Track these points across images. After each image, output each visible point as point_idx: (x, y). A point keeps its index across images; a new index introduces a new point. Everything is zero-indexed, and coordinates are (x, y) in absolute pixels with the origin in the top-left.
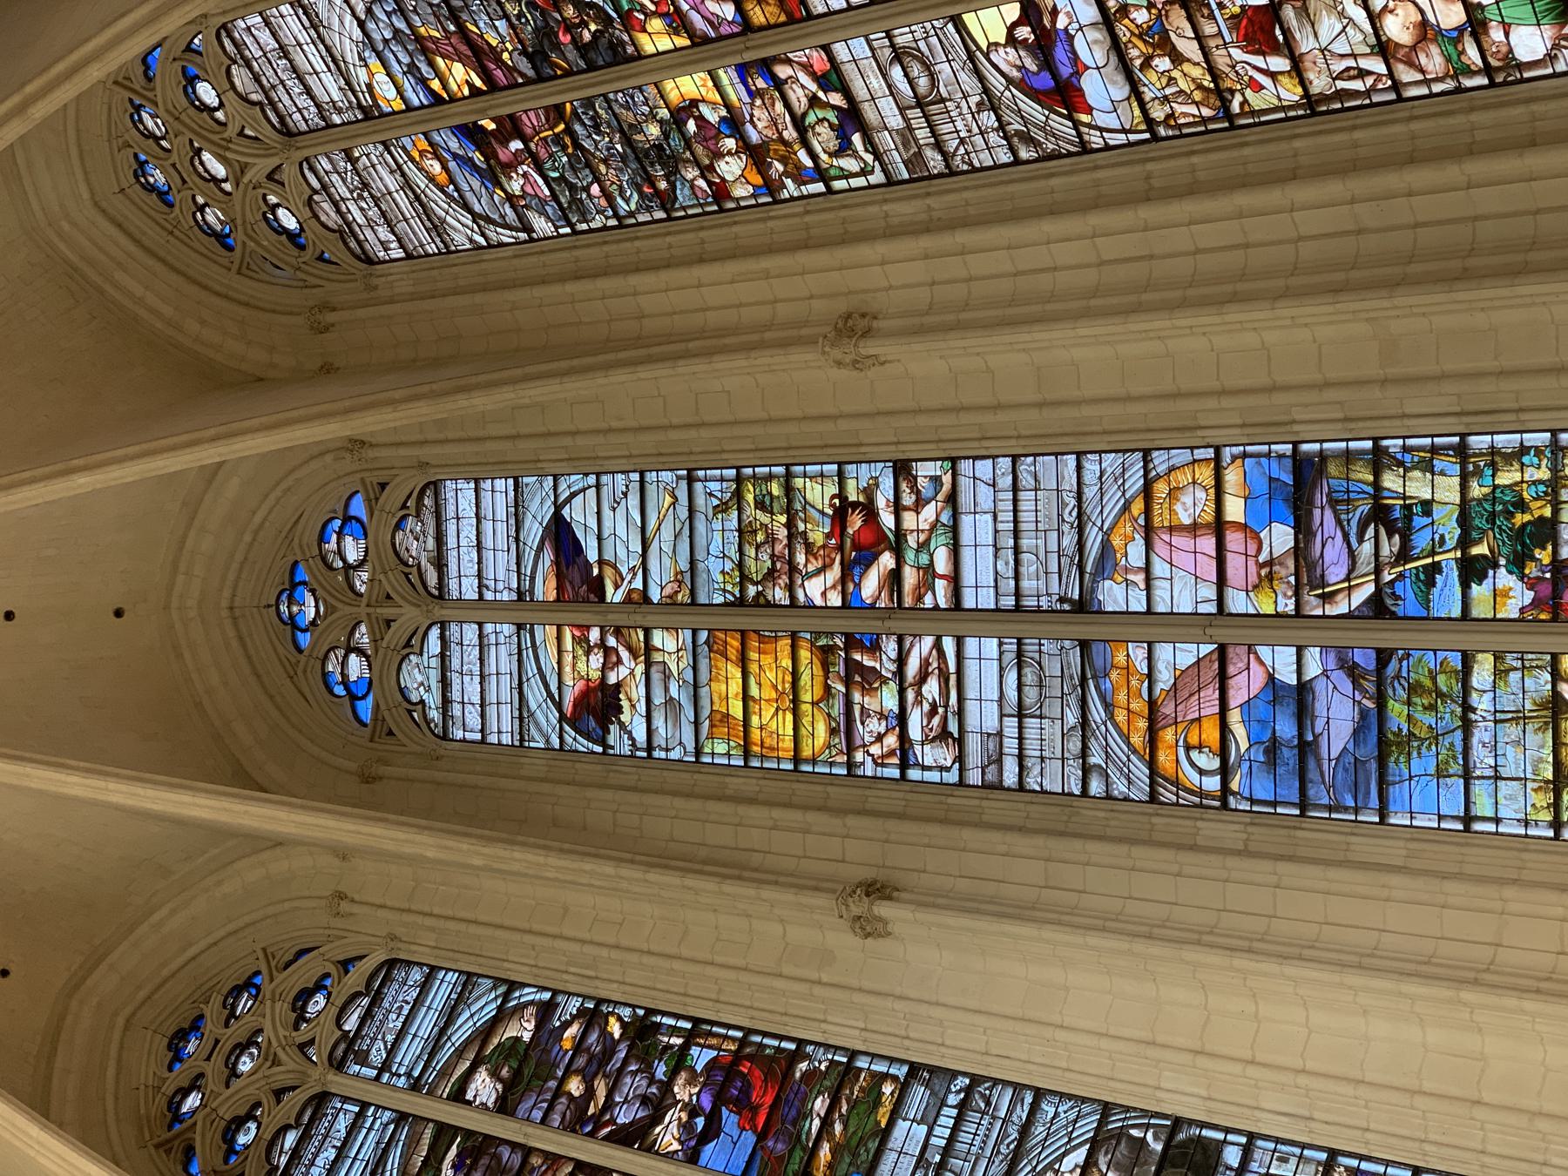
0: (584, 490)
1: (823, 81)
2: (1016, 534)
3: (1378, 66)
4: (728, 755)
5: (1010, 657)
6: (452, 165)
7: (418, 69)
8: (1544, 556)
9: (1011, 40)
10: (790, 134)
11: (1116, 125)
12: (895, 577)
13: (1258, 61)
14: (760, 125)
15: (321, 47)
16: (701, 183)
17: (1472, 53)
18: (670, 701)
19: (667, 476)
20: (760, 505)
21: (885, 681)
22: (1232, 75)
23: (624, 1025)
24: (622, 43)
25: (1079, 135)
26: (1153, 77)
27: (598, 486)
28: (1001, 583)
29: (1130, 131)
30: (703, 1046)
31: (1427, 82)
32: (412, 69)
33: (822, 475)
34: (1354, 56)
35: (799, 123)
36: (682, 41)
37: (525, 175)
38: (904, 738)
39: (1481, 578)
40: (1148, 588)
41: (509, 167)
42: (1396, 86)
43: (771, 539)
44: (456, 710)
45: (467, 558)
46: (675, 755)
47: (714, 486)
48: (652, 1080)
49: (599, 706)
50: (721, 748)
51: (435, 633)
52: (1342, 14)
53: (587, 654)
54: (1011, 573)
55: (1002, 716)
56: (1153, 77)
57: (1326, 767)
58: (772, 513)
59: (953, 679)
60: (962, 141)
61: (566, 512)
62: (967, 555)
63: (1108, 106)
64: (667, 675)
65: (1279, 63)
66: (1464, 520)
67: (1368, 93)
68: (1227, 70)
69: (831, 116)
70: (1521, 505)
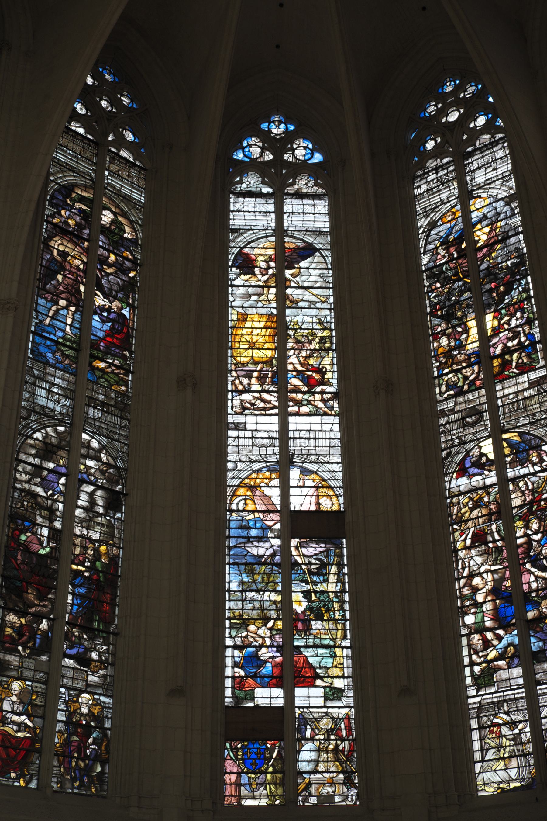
0: (326, 263)
1: (473, 382)
2: (315, 439)
4: (232, 320)
5: (272, 434)
6: (449, 225)
7: (485, 220)
8: (312, 617)
9: (482, 455)
10: (455, 367)
11: (452, 486)
12: (297, 390)
13: (470, 536)
14: (458, 356)
15: (495, 179)
16: (439, 329)
17: (468, 603)
18: (250, 296)
19: (331, 300)
20: (322, 338)
21: (261, 386)
22: (466, 527)
23: (133, 277)
24: (490, 309)
25: (449, 473)
27: (328, 269)
28: (298, 433)
29: (449, 491)
30: (130, 312)
31: (460, 589)
32: (485, 217)
33: (333, 364)
34: (469, 567)
35: (459, 371)
36: (489, 333)
37: (444, 257)
38: (241, 392)
39: (305, 597)
40: (298, 487)
41: (447, 249)
42: (459, 579)
43: (310, 342)
44: (241, 200)
45: (299, 208)
46: (231, 298)
47: (328, 319)
48: (117, 292)
49: (247, 265)
50: (235, 317)
51: (270, 190)
52: (482, 564)
53: (265, 261)
54: (301, 436)
55: (252, 431)
56: (466, 500)
57: (242, 545)
58: (319, 343)
59: (263, 412)
60: (450, 431)
61: (317, 254)
62: (306, 419)
63: (458, 484)
64: (259, 295)
65: (468, 542)
66: (322, 592)
67: (458, 570)
69: (460, 384)
70: (328, 610)
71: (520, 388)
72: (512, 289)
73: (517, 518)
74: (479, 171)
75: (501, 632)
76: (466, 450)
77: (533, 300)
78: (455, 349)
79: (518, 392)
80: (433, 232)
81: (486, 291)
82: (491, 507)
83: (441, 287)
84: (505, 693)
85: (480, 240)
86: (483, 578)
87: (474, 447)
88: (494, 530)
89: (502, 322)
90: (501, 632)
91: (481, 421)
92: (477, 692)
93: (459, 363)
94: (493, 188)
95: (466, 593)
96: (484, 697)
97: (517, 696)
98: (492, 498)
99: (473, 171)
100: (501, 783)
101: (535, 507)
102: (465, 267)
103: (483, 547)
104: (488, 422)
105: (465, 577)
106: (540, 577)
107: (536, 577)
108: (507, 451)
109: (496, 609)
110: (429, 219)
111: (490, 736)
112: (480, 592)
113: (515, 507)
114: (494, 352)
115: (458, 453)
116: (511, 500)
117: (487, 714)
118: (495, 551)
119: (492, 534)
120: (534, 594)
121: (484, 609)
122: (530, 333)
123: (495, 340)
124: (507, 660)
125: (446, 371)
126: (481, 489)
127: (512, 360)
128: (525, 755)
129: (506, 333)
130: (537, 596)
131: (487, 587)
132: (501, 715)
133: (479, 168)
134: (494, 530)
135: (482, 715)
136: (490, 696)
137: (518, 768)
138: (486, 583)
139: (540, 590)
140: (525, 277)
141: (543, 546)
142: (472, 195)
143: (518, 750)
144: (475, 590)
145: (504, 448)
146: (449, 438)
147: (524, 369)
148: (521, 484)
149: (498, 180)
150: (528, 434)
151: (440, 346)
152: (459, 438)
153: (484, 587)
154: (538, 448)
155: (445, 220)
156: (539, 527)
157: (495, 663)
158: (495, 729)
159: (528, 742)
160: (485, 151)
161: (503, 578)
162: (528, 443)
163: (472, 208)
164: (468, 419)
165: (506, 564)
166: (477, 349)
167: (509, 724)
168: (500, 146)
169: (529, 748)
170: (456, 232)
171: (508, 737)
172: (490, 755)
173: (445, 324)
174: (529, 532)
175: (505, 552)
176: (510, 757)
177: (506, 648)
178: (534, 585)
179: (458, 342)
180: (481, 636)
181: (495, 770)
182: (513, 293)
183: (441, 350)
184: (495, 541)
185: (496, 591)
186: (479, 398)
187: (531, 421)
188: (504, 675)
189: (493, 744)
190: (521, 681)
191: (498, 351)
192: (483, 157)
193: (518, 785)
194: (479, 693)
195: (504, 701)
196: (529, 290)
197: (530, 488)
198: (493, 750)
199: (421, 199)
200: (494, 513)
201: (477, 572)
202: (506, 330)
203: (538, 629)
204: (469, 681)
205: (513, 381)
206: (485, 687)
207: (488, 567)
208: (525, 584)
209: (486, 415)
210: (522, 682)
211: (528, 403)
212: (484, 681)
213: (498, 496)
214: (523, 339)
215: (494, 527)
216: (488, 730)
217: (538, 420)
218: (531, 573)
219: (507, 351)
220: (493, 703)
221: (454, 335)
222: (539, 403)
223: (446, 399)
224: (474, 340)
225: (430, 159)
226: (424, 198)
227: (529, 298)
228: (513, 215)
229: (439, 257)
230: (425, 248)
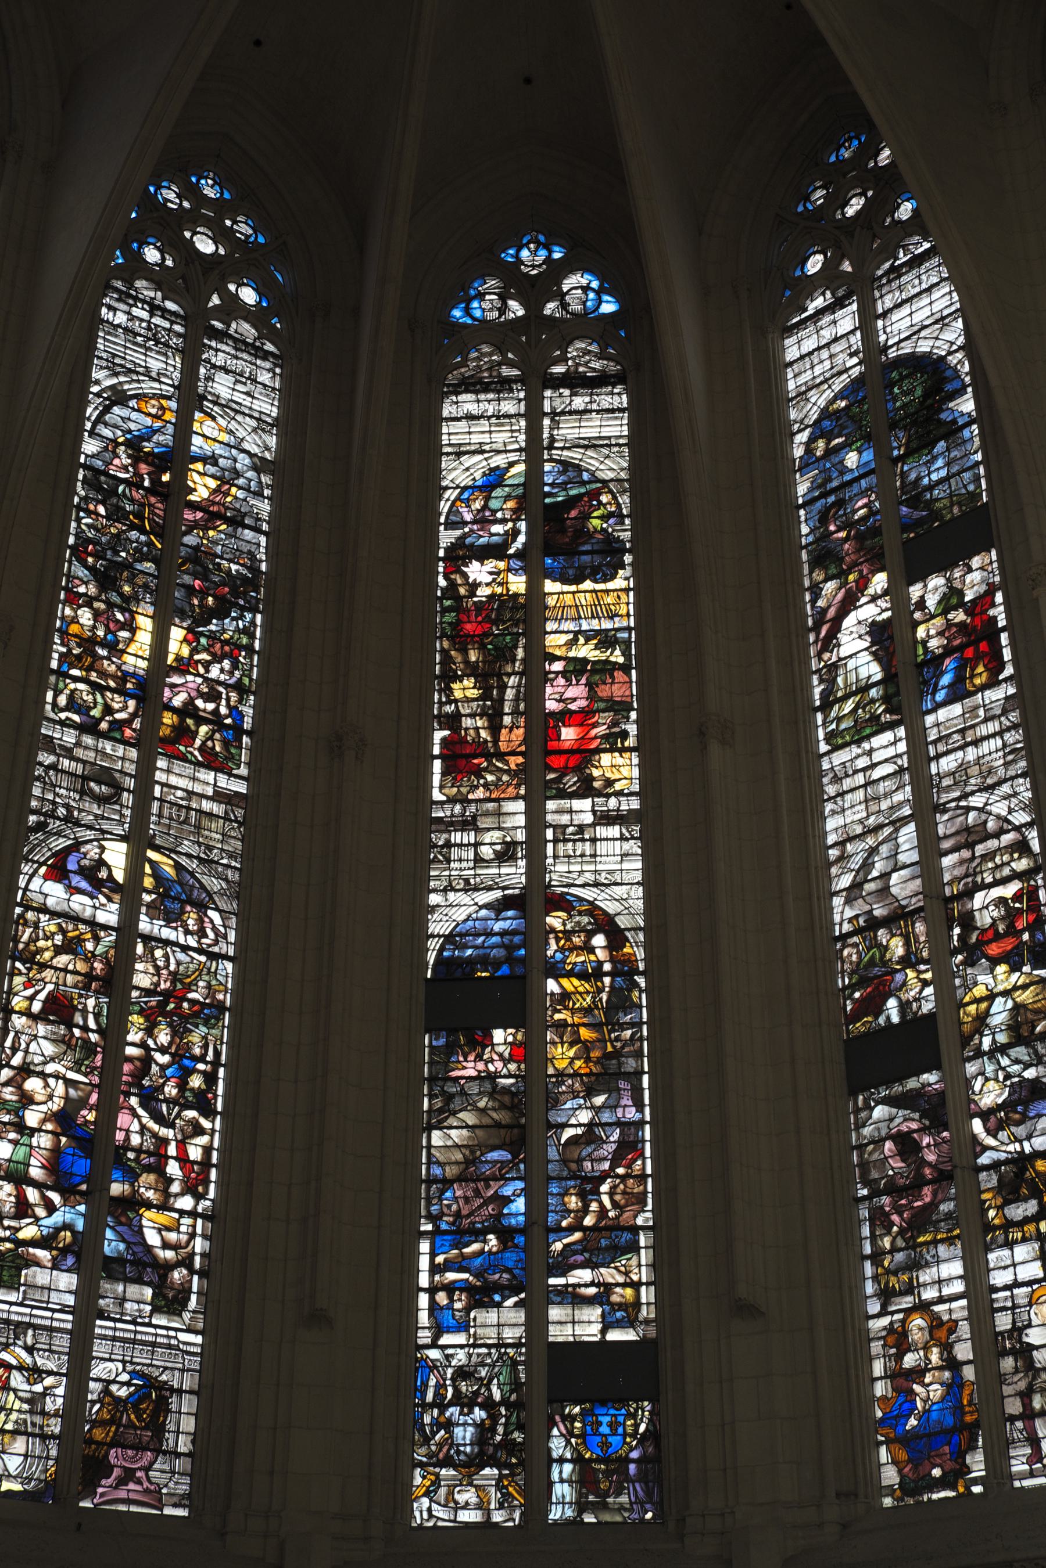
1: (118, 726)
3: (16, 1061)
9: (101, 863)
13: (42, 996)
14: (106, 663)
16: (82, 589)
22: (38, 976)
24: (182, 620)
25: (34, 862)
26: (53, 928)
29: (24, 894)
32: (212, 460)
37: (125, 468)
52: (52, 1059)
56: (53, 928)
60: (55, 786)
63: (45, 890)
65: (37, 1006)
68: (43, 975)
69: (96, 713)
71: (198, 788)
72: (228, 615)
73: (137, 1008)
74: (222, 375)
75: (55, 1197)
76: (75, 838)
77: (256, 658)
78: (103, 644)
79: (193, 793)
80: (116, 409)
81: (183, 586)
82: (96, 965)
83: (108, 517)
84: (35, 1312)
85: (195, 490)
86: (47, 1085)
87: (91, 841)
88: (91, 1009)
89: (196, 657)
90: (55, 1197)
91: (115, 803)
93: (103, 674)
94: (239, 423)
95: (8, 1097)
97: (55, 1324)
98: (100, 949)
99: (214, 366)
101: (172, 1006)
102: (158, 516)
103: (62, 1030)
104: (127, 812)
105: (12, 1067)
106: (149, 1130)
107: (143, 1128)
108: (148, 882)
109: (56, 1151)
110: (115, 381)
112: (34, 1107)
113: (137, 988)
114: (171, 699)
115: (59, 834)
116: (132, 971)
118: (82, 1047)
119: (85, 1012)
120: (131, 1155)
121: (34, 1141)
122: (236, 708)
123: (176, 679)
124: (54, 1253)
125: (75, 672)
126: (85, 922)
127: (197, 732)
128: (44, 1437)
129: (199, 680)
130: (137, 1160)
131: (50, 1103)
132: (18, 1350)
133: (227, 372)
134: (91, 1009)
137: (26, 1456)
138: (50, 1097)
139: (145, 1152)
140: (254, 610)
141: (168, 1079)
142: (202, 405)
143: (34, 1424)
144: (27, 1100)
145: (143, 874)
146: (50, 797)
147: (211, 762)
148: (158, 953)
149: (251, 417)
150: (192, 874)
151: (75, 620)
152: (67, 806)
153: (45, 1103)
154: (202, 908)
155: (143, 405)
156: (170, 1044)
157: (31, 1250)
159: (56, 1415)
160: (243, 351)
161: (83, 1103)
162: (187, 888)
163: (196, 426)
164: (92, 784)
165: (96, 1080)
166: (142, 672)
167: (28, 1369)
168: (268, 365)
169: (55, 1427)
170: (159, 444)
171: (20, 1394)
173: (96, 587)
174: (150, 1042)
175: (99, 1057)
176: (15, 1433)
177: (58, 1230)
178: (135, 1140)
179: (109, 637)
180: (17, 1188)
182: (227, 621)
183: (74, 629)
184: (85, 1029)
185: (64, 1119)
186: (123, 759)
187: (203, 856)
188: (42, 1277)
190: (70, 1300)
191: (178, 701)
192: (237, 358)
193: (17, 1487)
196: (252, 636)
197: (172, 967)
199: (109, 333)
200: (97, 978)
201: (39, 1069)
202: (198, 675)
203: (123, 1220)
205: (189, 770)
207: (63, 1070)
208: (121, 1129)
209: (127, 798)
211: (205, 822)
213: (112, 952)
214: (223, 710)
215: (91, 1003)
217: (212, 861)
218: (135, 1114)
219: (188, 710)
221: (108, 619)
222: (223, 835)
223: (62, 723)
224: (140, 653)
225: (147, 280)
226: (116, 336)
227: (250, 650)
228: (259, 494)
229: (116, 462)
230: (95, 425)
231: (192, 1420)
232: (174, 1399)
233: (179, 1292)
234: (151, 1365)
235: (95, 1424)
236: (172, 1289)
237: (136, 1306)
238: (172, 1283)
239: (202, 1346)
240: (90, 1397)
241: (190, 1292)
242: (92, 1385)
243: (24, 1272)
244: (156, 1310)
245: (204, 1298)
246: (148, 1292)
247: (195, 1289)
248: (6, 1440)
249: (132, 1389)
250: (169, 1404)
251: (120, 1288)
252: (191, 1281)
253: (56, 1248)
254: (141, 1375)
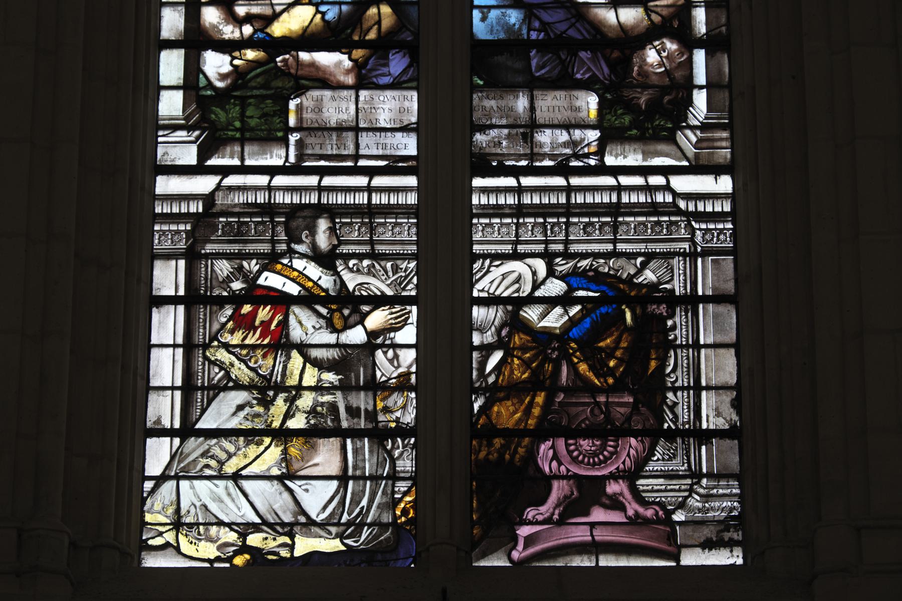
84: (328, 181)
92: (204, 152)
96: (232, 180)
100: (255, 528)
111: (236, 339)
117: (235, 248)
124: (358, 53)
128: (380, 435)
132: (299, 264)
135: (209, 248)
136: (262, 180)
137: (343, 479)
143: (353, 412)
157: (304, 56)
158: (264, 313)
159: (403, 384)
167: (326, 300)
169: (404, 410)
171: (315, 353)
172: (221, 413)
181: (236, 477)
188: (337, 108)
189: (241, 372)
190: (408, 145)
194: (213, 162)
195: (320, 210)
198: (241, 397)
204: (171, 104)
206: (242, 142)
210: (412, 151)
212: (242, 117)
216: (228, 311)
220: (269, 209)
231: (729, 359)
232: (679, 318)
233: (664, 90)
234: (615, 254)
235: (494, 394)
236: (645, 86)
237: (563, 136)
238: (643, 73)
239: (732, 197)
240: (476, 339)
241: (689, 86)
242: (478, 313)
243: (292, 105)
244: (611, 136)
245: (724, 96)
246: (590, 103)
247: (700, 77)
248: (293, 451)
249: (575, 310)
250: (667, 331)
251: (522, 103)
252: (690, 62)
253: (362, 44)
254: (594, 278)
